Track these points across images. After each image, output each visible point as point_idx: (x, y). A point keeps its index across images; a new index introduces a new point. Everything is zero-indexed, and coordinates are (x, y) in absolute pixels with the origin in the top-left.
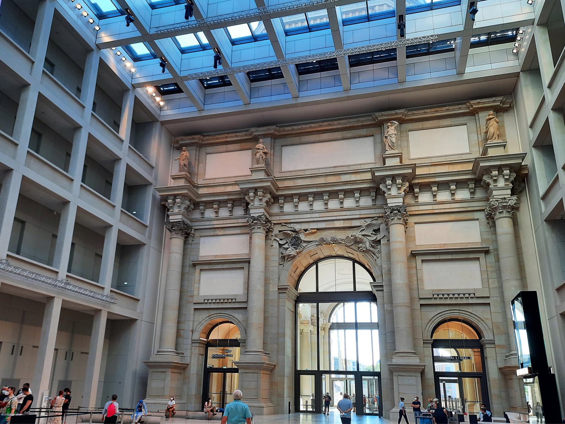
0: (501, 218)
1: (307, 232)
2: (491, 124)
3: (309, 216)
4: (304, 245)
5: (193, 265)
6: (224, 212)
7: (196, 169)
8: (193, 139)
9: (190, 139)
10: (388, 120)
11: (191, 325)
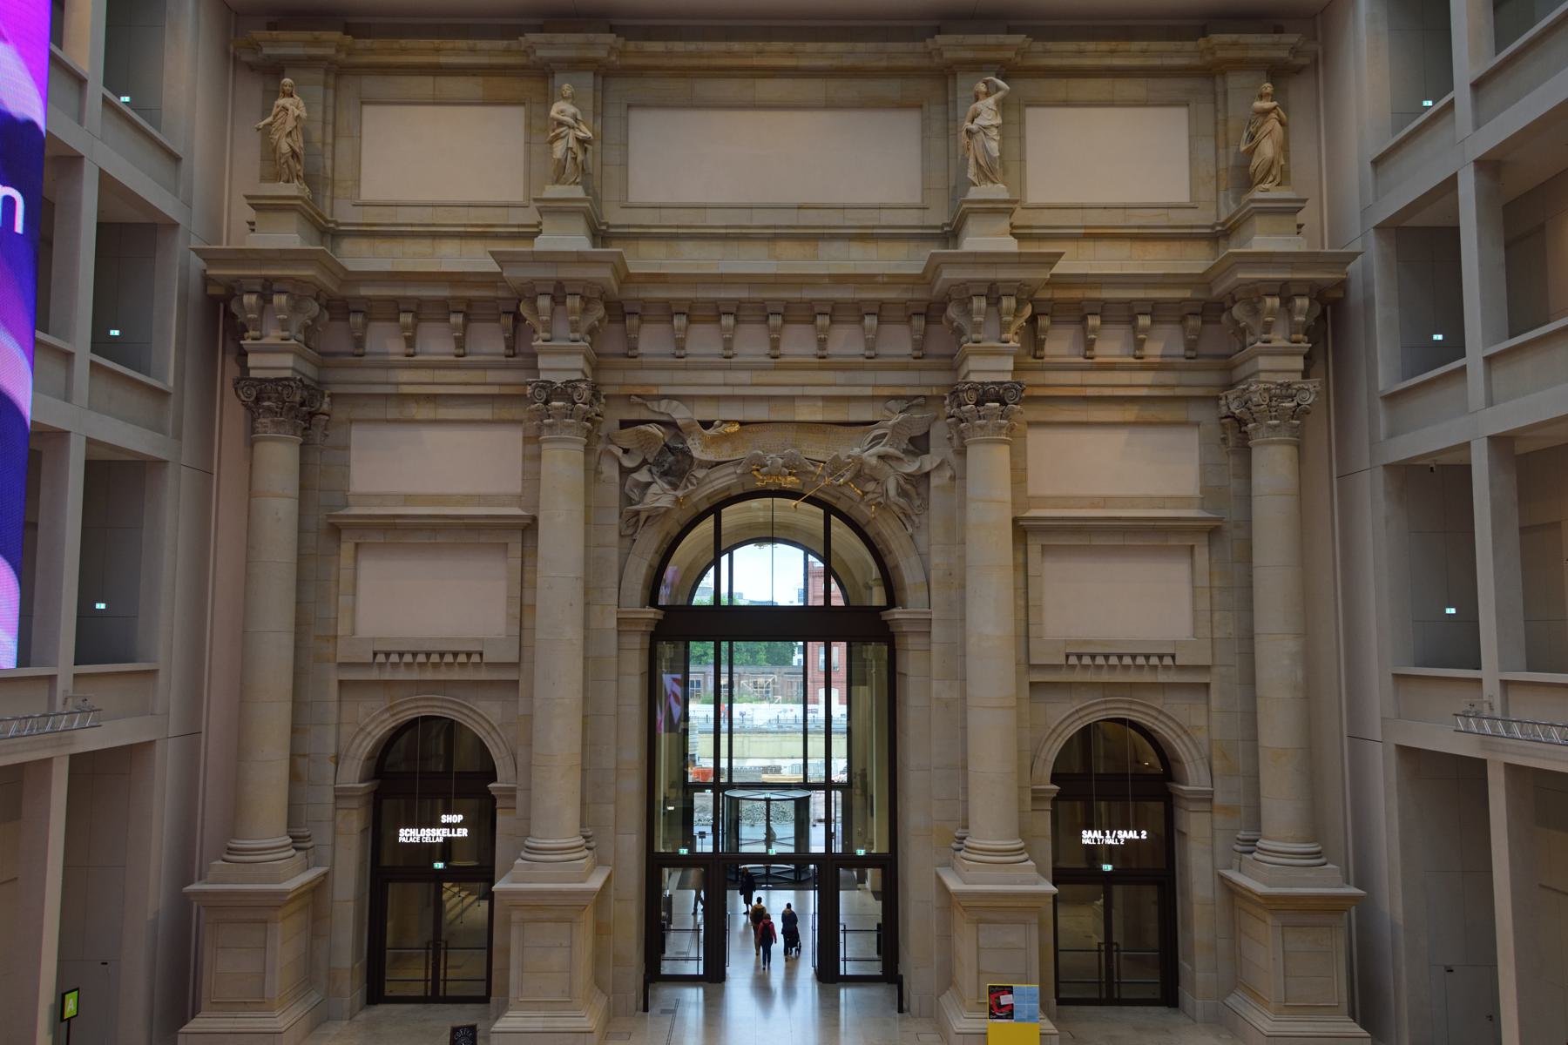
0: (1273, 443)
1: (711, 432)
2: (1267, 127)
3: (718, 377)
4: (700, 474)
5: (335, 532)
6: (436, 342)
7: (329, 163)
8: (317, 42)
9: (307, 43)
10: (977, 66)
11: (331, 741)
